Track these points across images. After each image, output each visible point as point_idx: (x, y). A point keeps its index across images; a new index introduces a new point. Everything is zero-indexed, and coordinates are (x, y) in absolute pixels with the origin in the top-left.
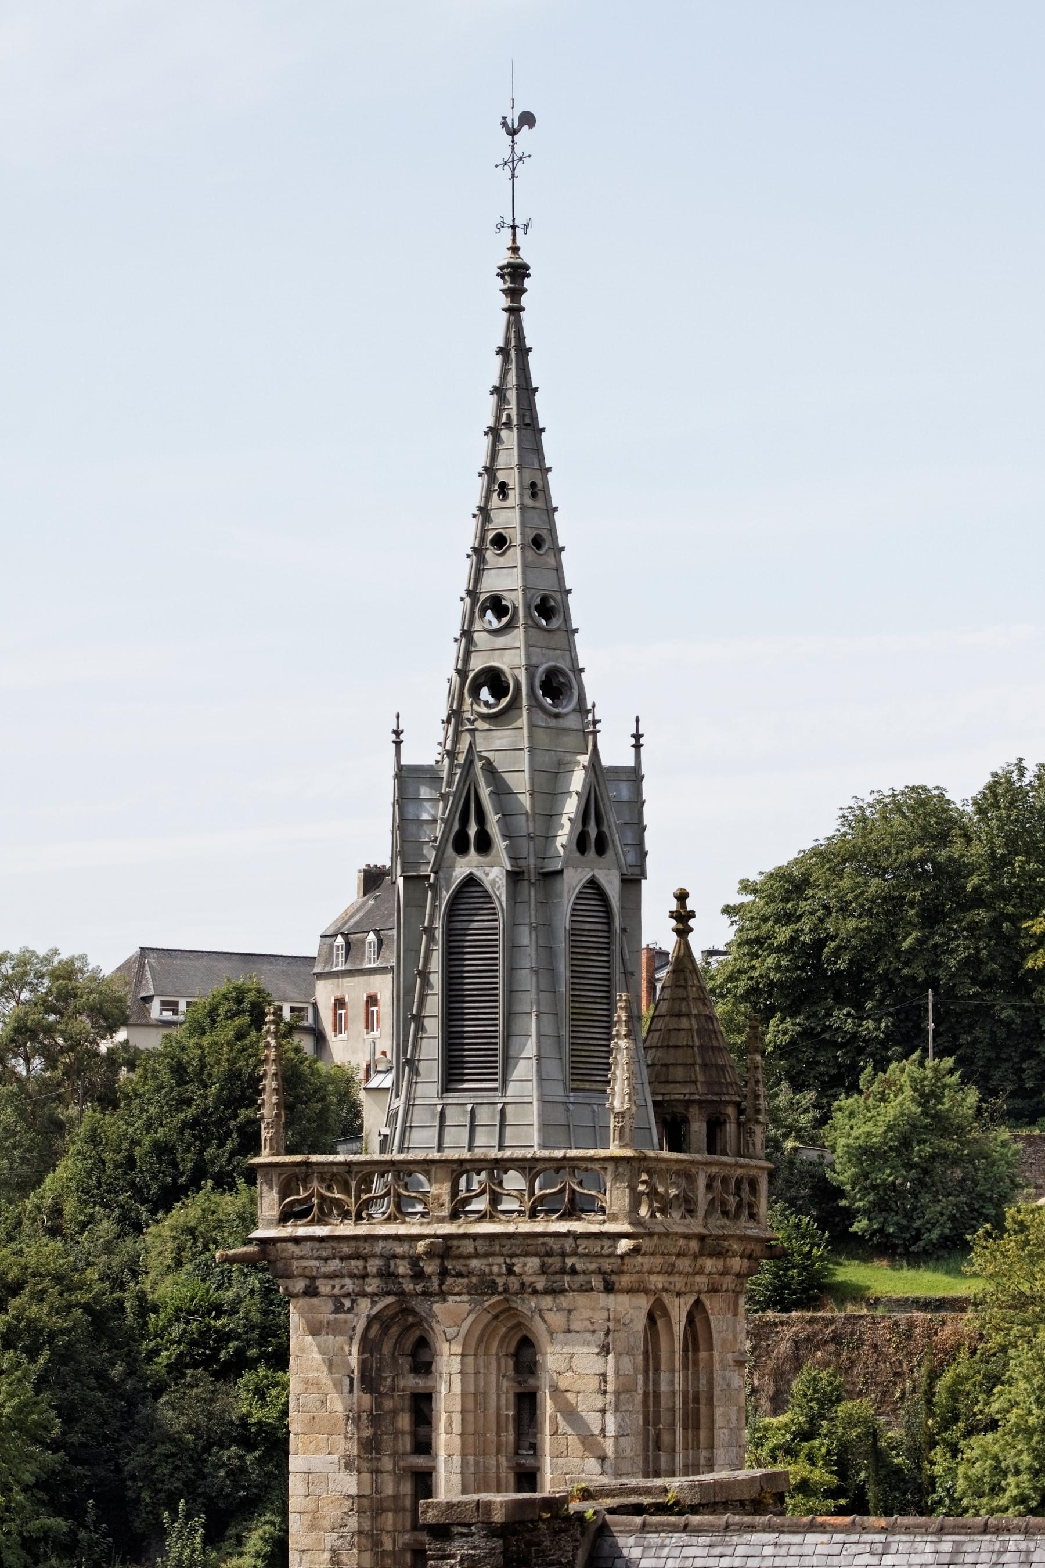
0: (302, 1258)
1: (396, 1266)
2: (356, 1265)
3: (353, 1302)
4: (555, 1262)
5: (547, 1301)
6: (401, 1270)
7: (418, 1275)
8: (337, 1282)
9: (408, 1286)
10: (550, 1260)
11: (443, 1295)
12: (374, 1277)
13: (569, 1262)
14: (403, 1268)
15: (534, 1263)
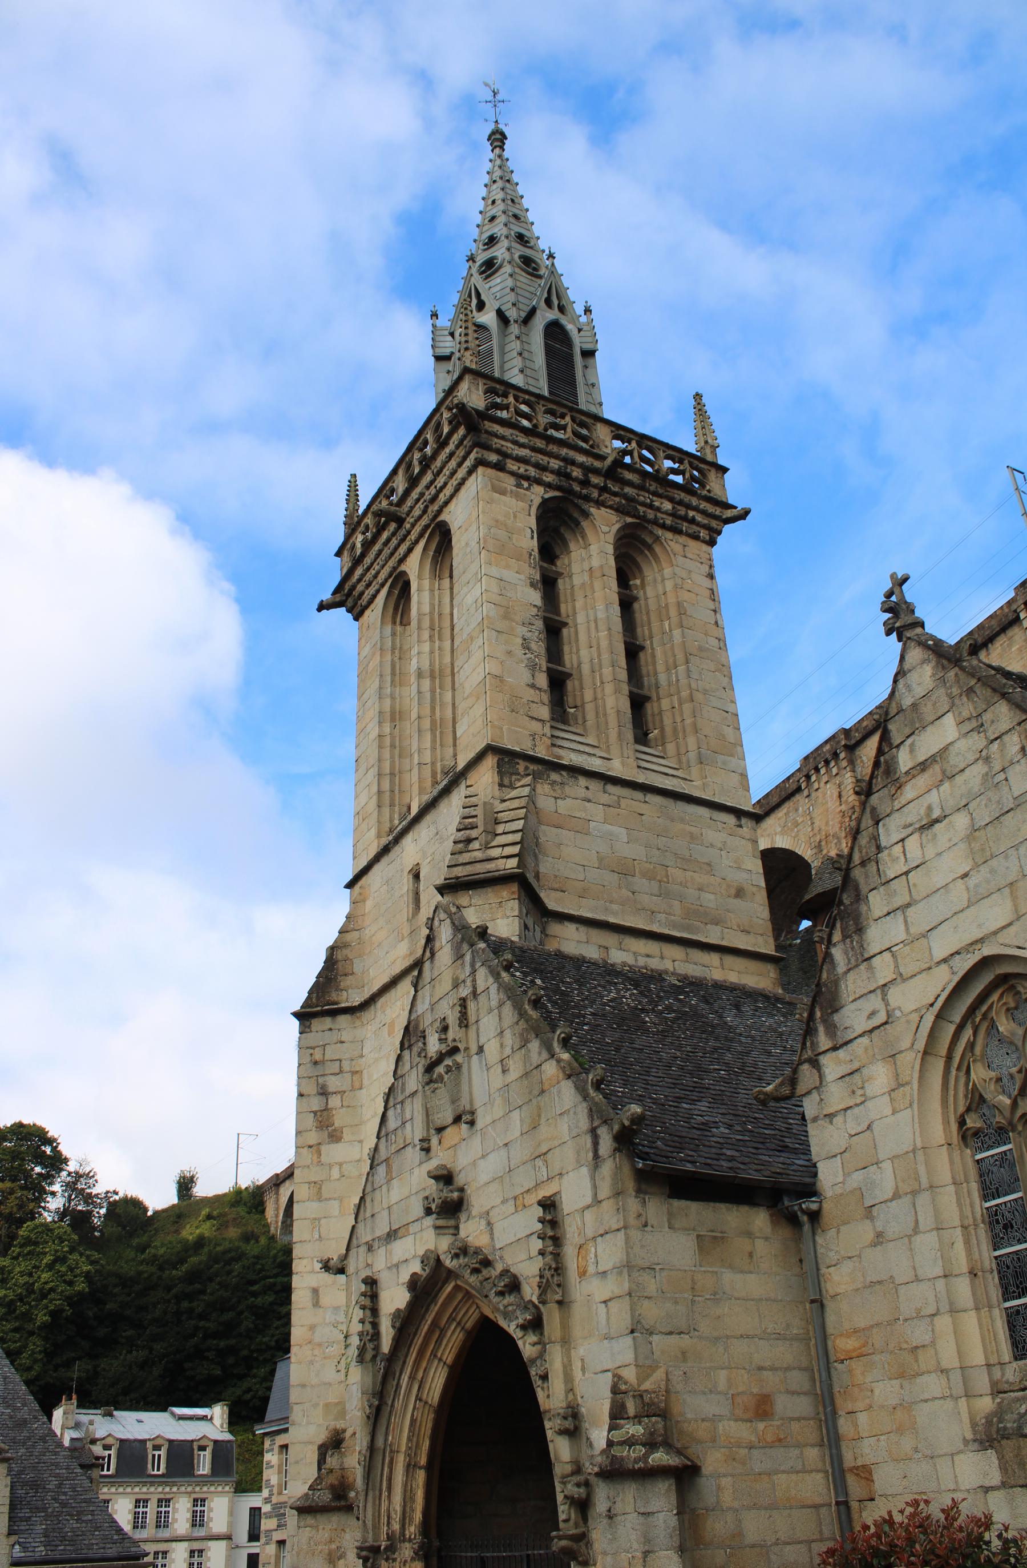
0: (503, 438)
1: (572, 471)
2: (543, 459)
3: (530, 485)
4: (682, 511)
5: (669, 535)
6: (574, 474)
7: (585, 483)
8: (521, 465)
9: (577, 488)
10: (679, 508)
11: (599, 504)
12: (552, 472)
13: (691, 513)
14: (577, 473)
15: (667, 506)
